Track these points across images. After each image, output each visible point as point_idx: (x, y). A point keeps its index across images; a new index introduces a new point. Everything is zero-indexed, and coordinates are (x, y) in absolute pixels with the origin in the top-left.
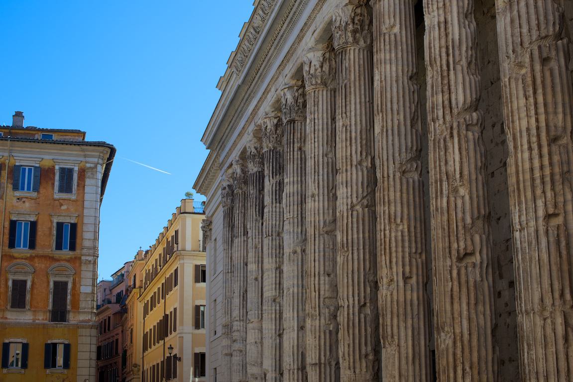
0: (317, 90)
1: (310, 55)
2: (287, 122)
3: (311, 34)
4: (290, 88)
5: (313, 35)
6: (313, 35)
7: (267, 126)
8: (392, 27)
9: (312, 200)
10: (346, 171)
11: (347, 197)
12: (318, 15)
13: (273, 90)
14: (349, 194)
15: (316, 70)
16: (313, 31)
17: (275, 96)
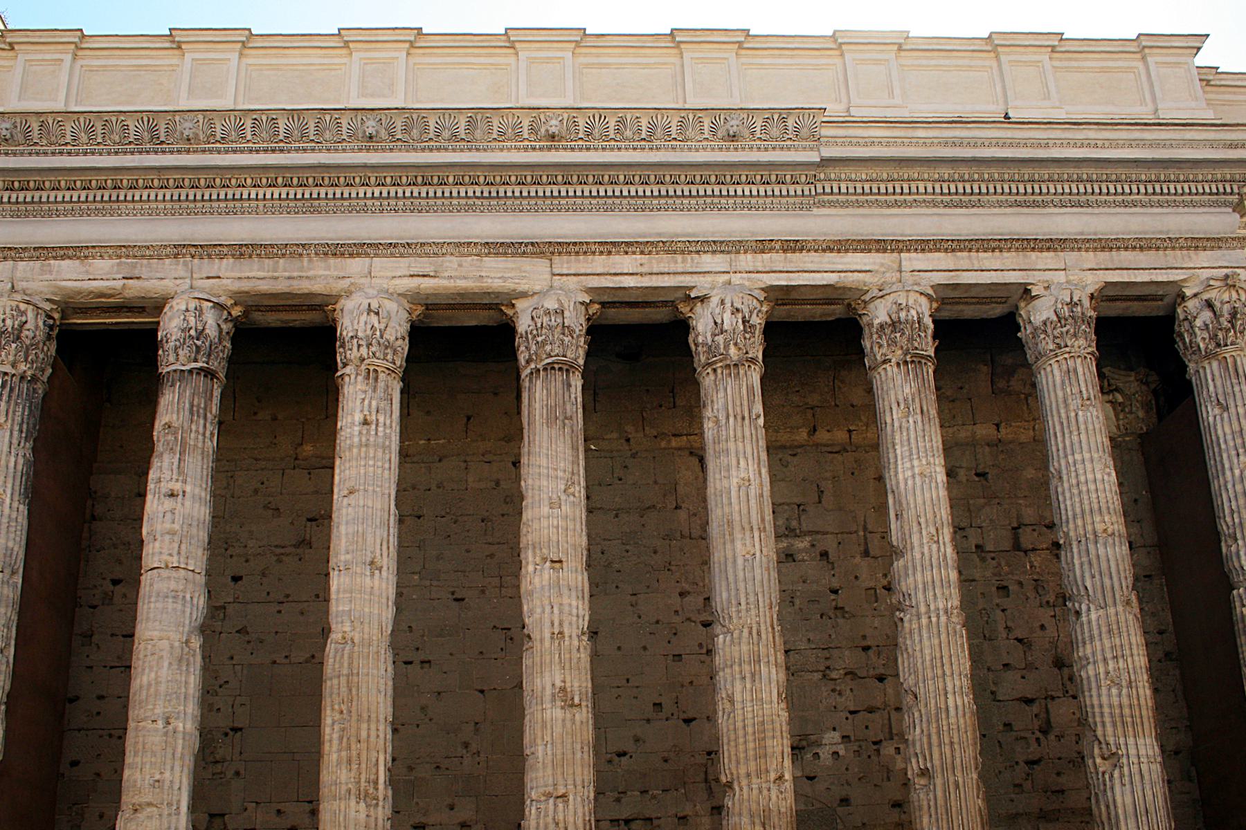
0: (393, 375)
1: (391, 306)
2: (201, 369)
4: (219, 306)
5: (412, 276)
6: (412, 276)
7: (26, 322)
8: (758, 416)
9: (372, 575)
10: (576, 571)
11: (578, 616)
12: (448, 258)
13: (102, 266)
14: (581, 612)
15: (397, 339)
16: (414, 271)
17: (118, 284)
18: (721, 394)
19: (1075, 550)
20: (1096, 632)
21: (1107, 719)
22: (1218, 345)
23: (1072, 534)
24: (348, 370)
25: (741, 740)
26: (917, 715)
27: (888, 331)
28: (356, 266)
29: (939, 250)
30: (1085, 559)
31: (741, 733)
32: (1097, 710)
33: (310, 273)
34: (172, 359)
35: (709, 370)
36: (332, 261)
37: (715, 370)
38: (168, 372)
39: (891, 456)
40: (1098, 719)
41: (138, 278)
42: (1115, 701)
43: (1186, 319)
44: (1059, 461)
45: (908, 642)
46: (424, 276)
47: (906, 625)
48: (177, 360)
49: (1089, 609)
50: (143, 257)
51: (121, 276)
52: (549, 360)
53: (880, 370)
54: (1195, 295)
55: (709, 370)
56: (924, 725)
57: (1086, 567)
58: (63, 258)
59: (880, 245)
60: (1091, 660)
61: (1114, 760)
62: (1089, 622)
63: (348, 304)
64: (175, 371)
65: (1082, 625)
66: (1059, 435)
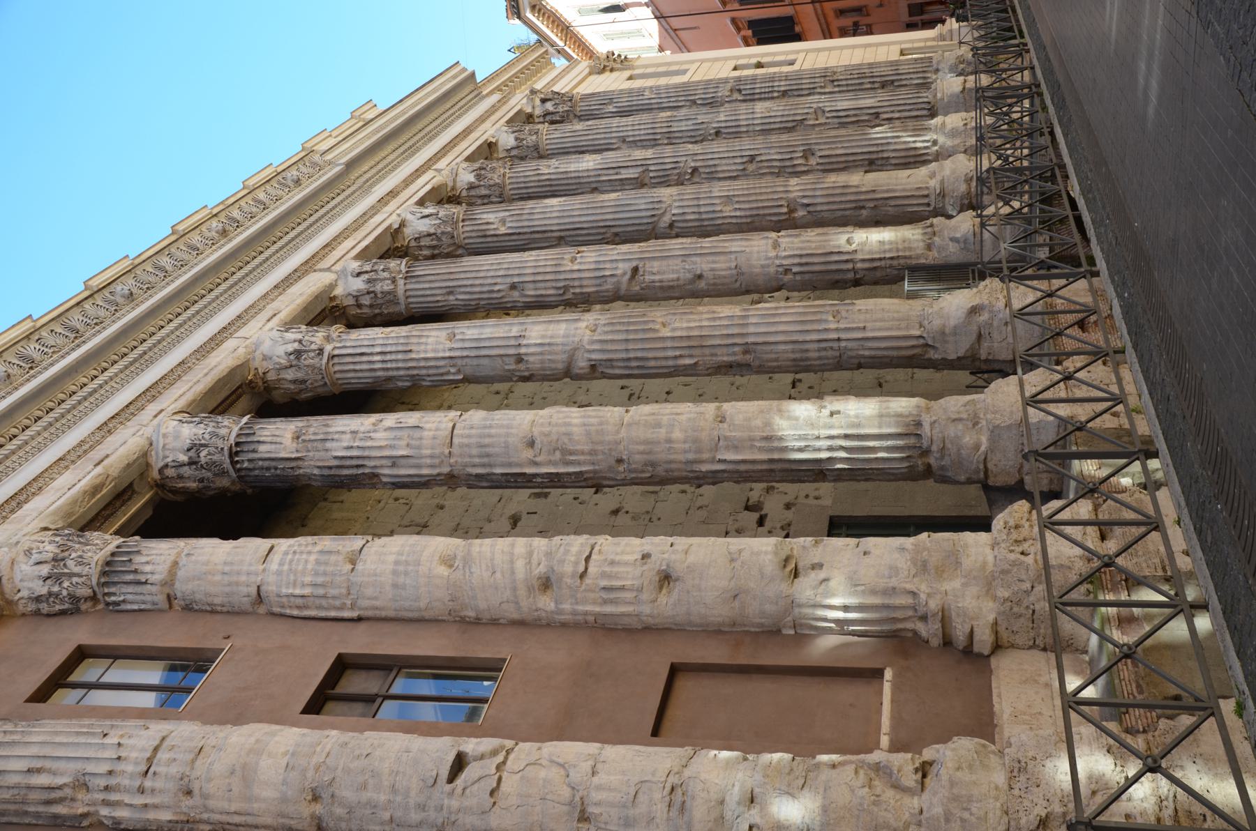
3: (260, 325)
5: (269, 320)
17: (99, 469)
18: (485, 216)
19: (675, 129)
20: (733, 118)
21: (792, 112)
22: (571, 100)
23: (664, 130)
24: (328, 348)
25: (758, 191)
26: (763, 158)
27: (483, 172)
28: (230, 344)
29: (439, 159)
30: (684, 123)
31: (752, 192)
32: (784, 119)
33: (213, 364)
34: (223, 432)
35: (461, 224)
36: (213, 354)
37: (463, 221)
38: (238, 435)
39: (573, 175)
40: (790, 119)
41: (107, 456)
42: (781, 108)
43: (545, 116)
44: (611, 138)
45: (711, 163)
46: (275, 315)
47: (698, 164)
48: (229, 428)
49: (718, 122)
50: (85, 452)
51: (92, 467)
52: (404, 263)
53: (508, 181)
54: (533, 108)
55: (461, 224)
56: (772, 151)
57: (690, 122)
58: (20, 505)
59: (418, 173)
60: (751, 122)
61: (820, 113)
62: (726, 121)
63: (266, 348)
64: (241, 429)
65: (726, 127)
66: (595, 137)
